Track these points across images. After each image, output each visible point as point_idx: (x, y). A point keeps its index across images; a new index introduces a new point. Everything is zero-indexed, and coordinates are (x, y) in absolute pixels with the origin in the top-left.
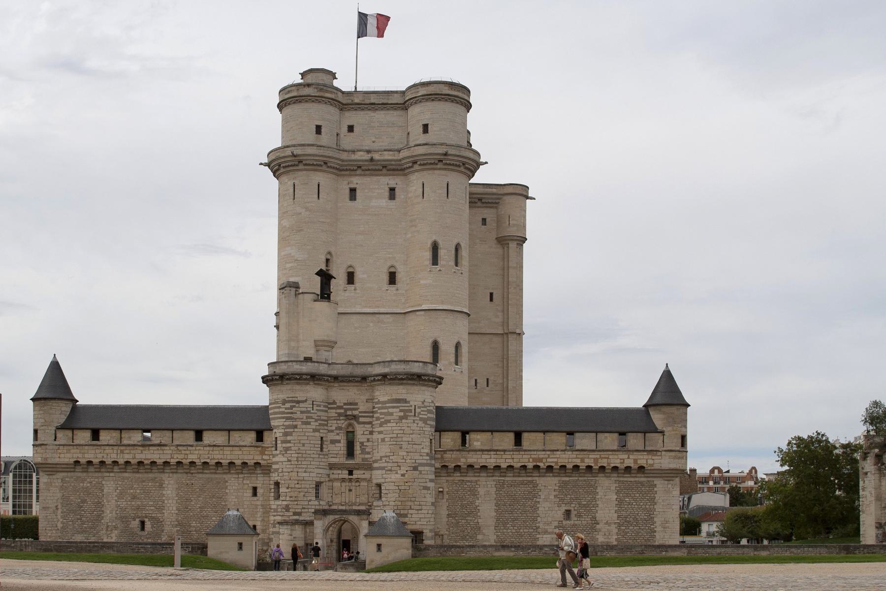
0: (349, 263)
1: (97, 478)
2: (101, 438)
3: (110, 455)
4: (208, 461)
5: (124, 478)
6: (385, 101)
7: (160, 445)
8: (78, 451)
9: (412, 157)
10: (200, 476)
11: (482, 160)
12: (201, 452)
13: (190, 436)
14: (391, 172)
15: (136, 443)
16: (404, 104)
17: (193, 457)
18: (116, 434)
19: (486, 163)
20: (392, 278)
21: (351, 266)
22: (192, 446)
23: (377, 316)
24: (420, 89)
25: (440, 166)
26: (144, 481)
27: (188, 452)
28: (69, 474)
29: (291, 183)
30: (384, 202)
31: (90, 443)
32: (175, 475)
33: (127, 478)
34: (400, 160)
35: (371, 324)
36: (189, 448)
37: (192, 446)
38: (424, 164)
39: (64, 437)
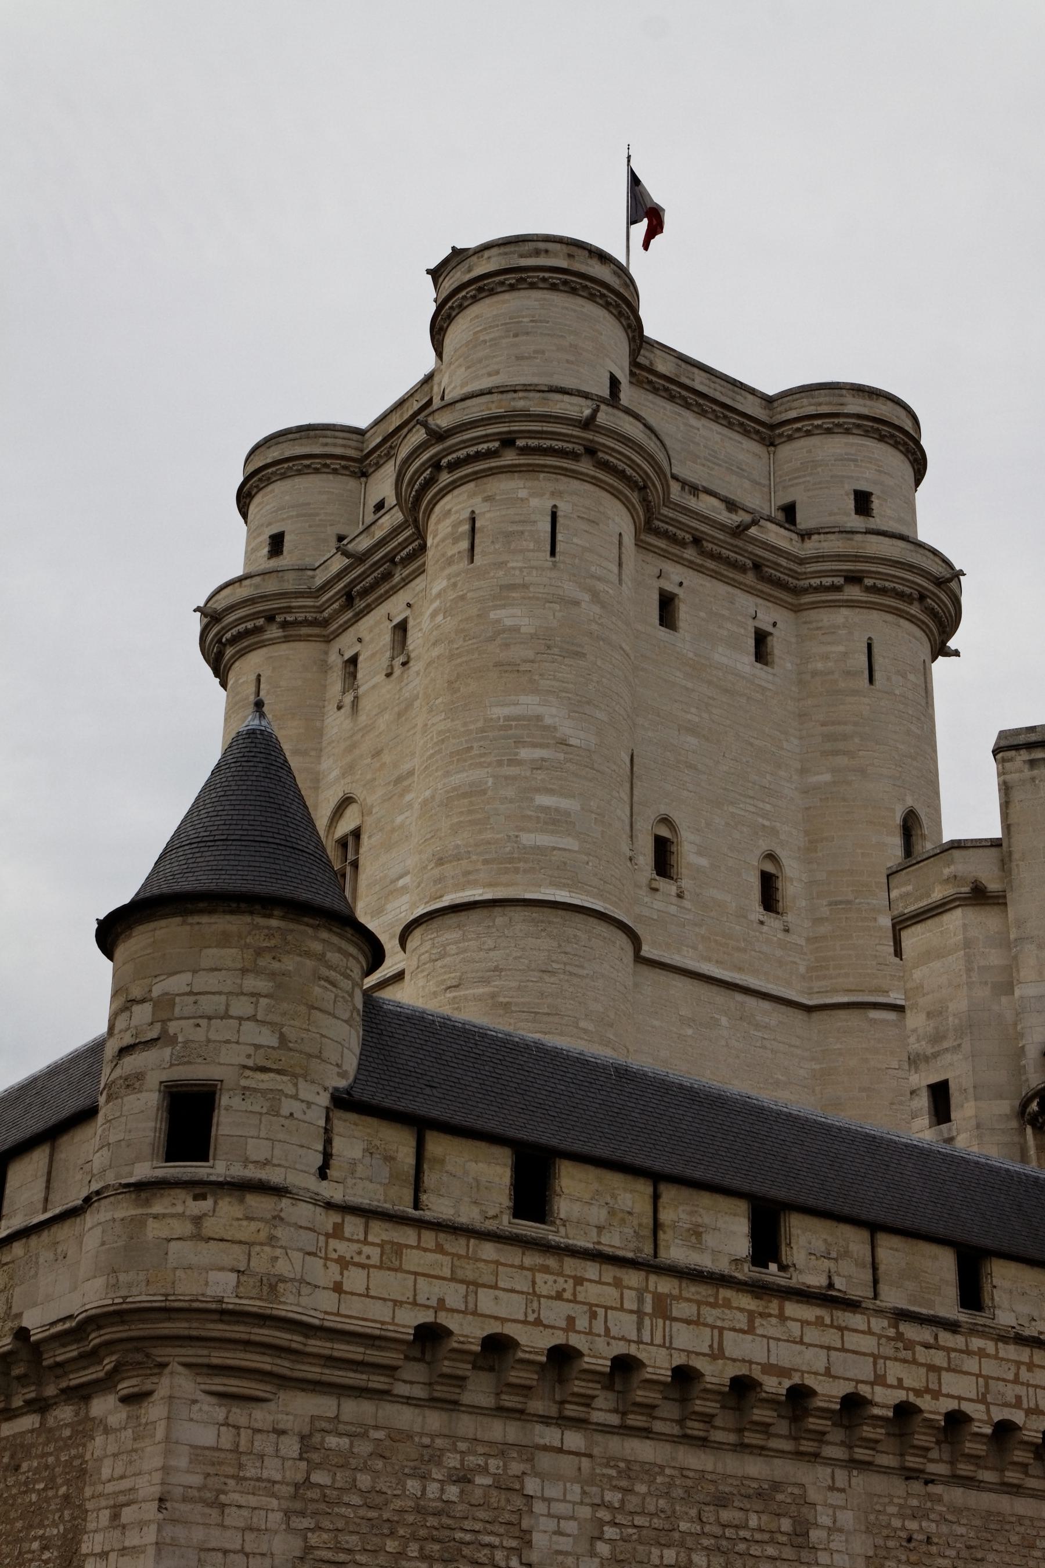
0: (663, 809)
1: (502, 1450)
2: (562, 1208)
3: (605, 1317)
4: (1018, 1417)
5: (630, 1470)
6: (729, 402)
7: (827, 1298)
8: (443, 1265)
9: (857, 558)
10: (957, 1495)
11: (952, 644)
12: (990, 1368)
13: (942, 1265)
14: (766, 588)
15: (723, 1266)
16: (772, 427)
17: (958, 1389)
18: (632, 1196)
19: (957, 653)
20: (770, 894)
21: (665, 820)
22: (952, 1327)
23: (739, 997)
24: (849, 398)
25: (914, 609)
26: (722, 1502)
27: (938, 1358)
28: (352, 1409)
29: (541, 505)
30: (745, 661)
31: (506, 1223)
32: (860, 1481)
33: (650, 1470)
34: (802, 561)
35: (724, 1021)
36: (946, 1338)
37: (952, 1327)
38: (883, 591)
39: (369, 1160)
